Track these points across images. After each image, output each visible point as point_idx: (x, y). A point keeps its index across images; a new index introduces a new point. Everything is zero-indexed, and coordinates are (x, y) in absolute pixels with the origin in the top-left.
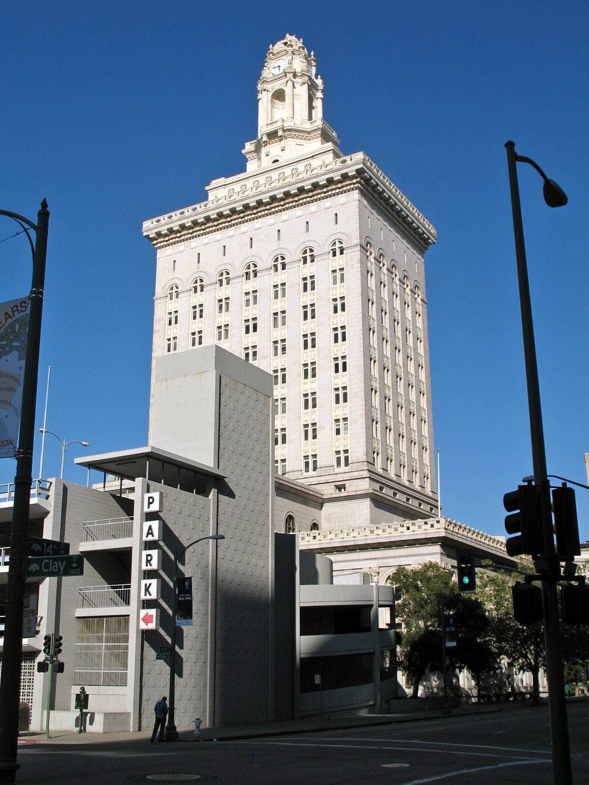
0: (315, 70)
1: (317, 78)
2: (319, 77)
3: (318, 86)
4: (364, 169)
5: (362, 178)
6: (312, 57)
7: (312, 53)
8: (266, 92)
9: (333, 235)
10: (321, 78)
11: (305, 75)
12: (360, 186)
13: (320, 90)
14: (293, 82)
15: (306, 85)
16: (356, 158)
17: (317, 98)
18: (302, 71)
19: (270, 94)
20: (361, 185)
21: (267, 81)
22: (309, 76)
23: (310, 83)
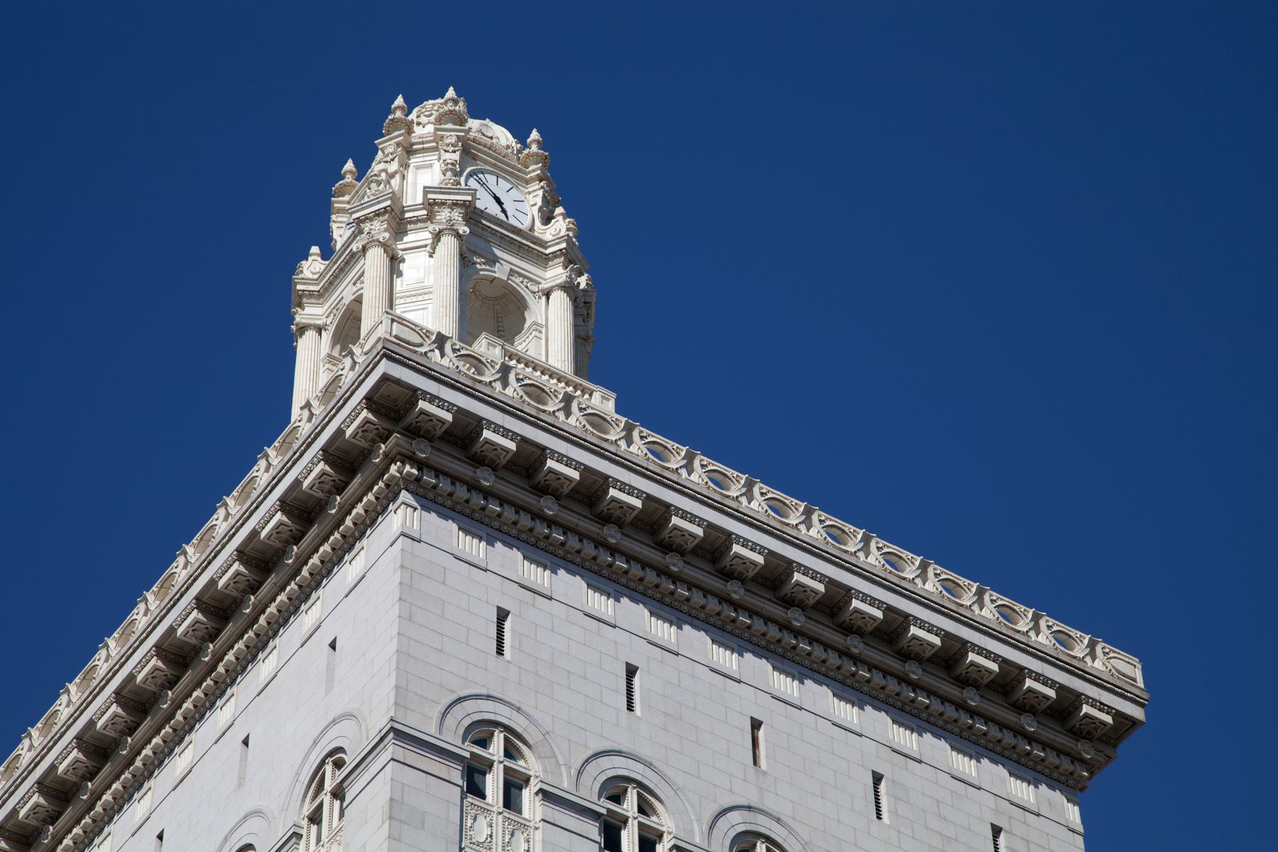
0: (541, 193)
1: (547, 219)
2: (560, 210)
3: (544, 244)
4: (398, 382)
5: (413, 432)
6: (534, 148)
7: (535, 135)
8: (310, 335)
9: (315, 743)
10: (566, 216)
11: (443, 204)
12: (408, 468)
13: (554, 255)
14: (385, 246)
15: (449, 245)
16: (366, 348)
17: (548, 295)
18: (427, 190)
19: (327, 337)
20: (420, 465)
21: (311, 294)
22: (464, 205)
23: (464, 229)
